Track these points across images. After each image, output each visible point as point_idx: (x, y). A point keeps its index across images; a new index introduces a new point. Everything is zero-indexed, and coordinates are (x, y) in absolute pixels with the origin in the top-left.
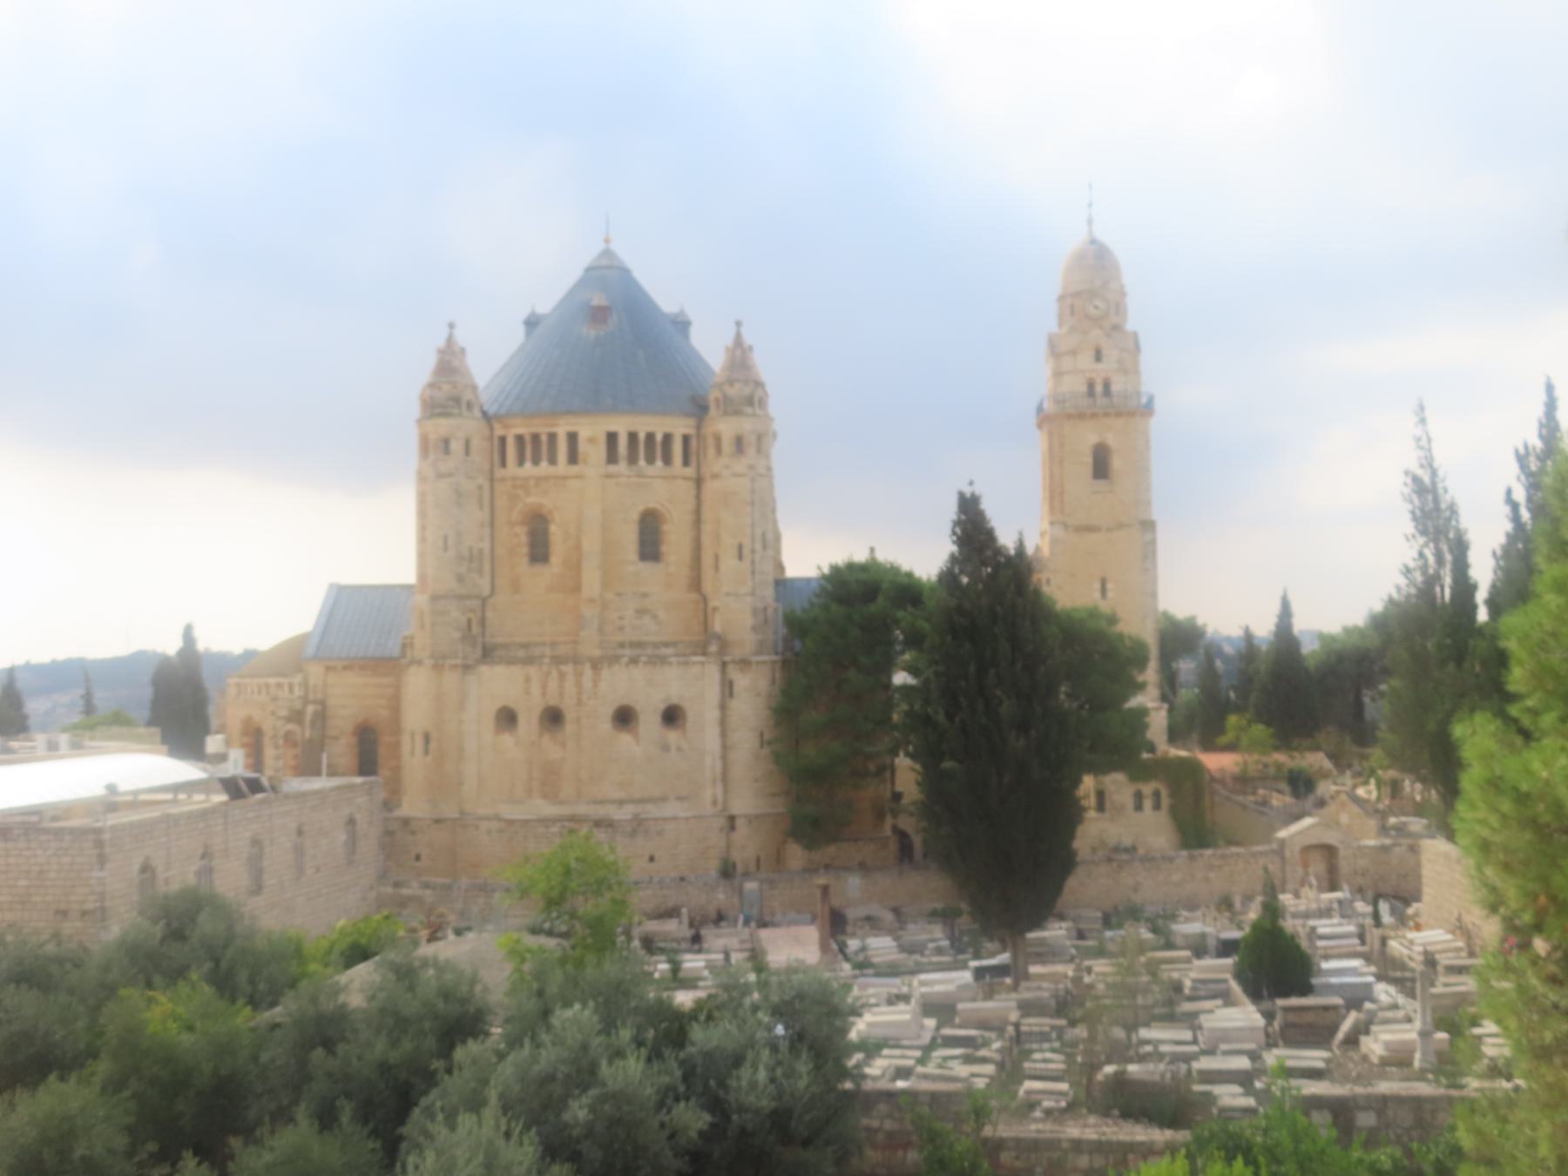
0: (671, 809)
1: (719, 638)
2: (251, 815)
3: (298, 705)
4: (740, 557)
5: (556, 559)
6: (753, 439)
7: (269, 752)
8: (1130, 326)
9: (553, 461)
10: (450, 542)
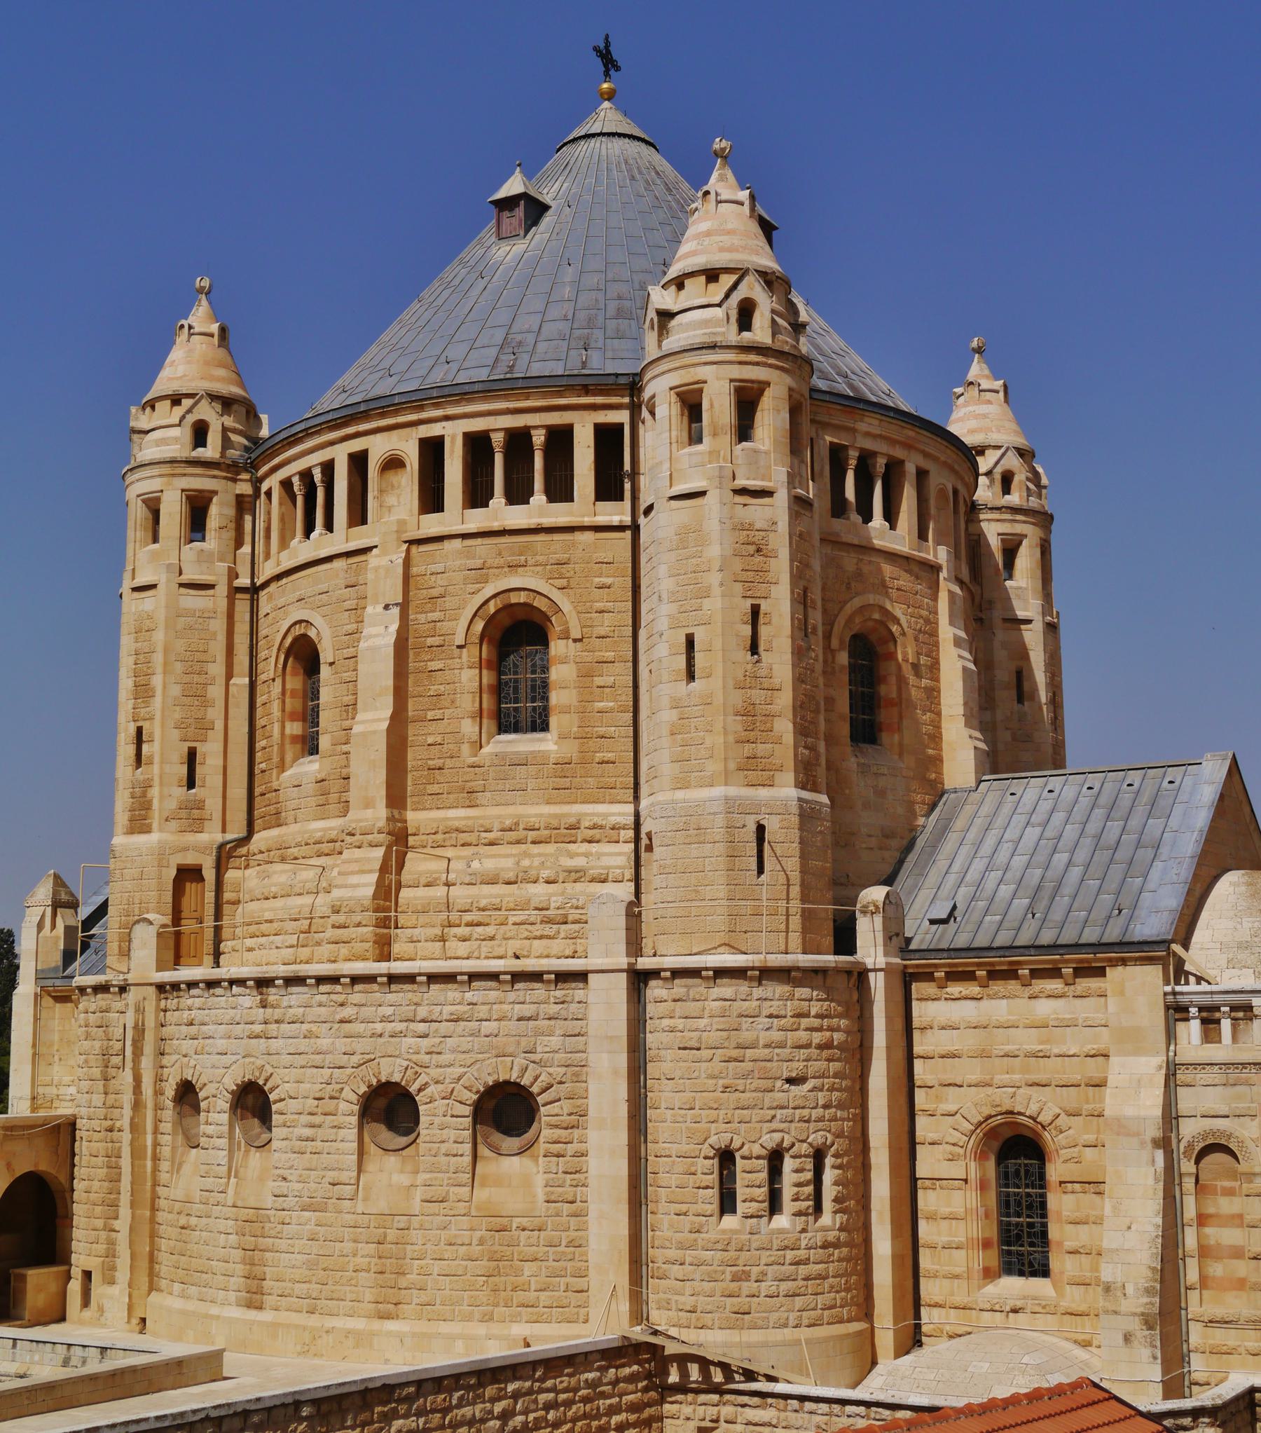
9: (329, 526)
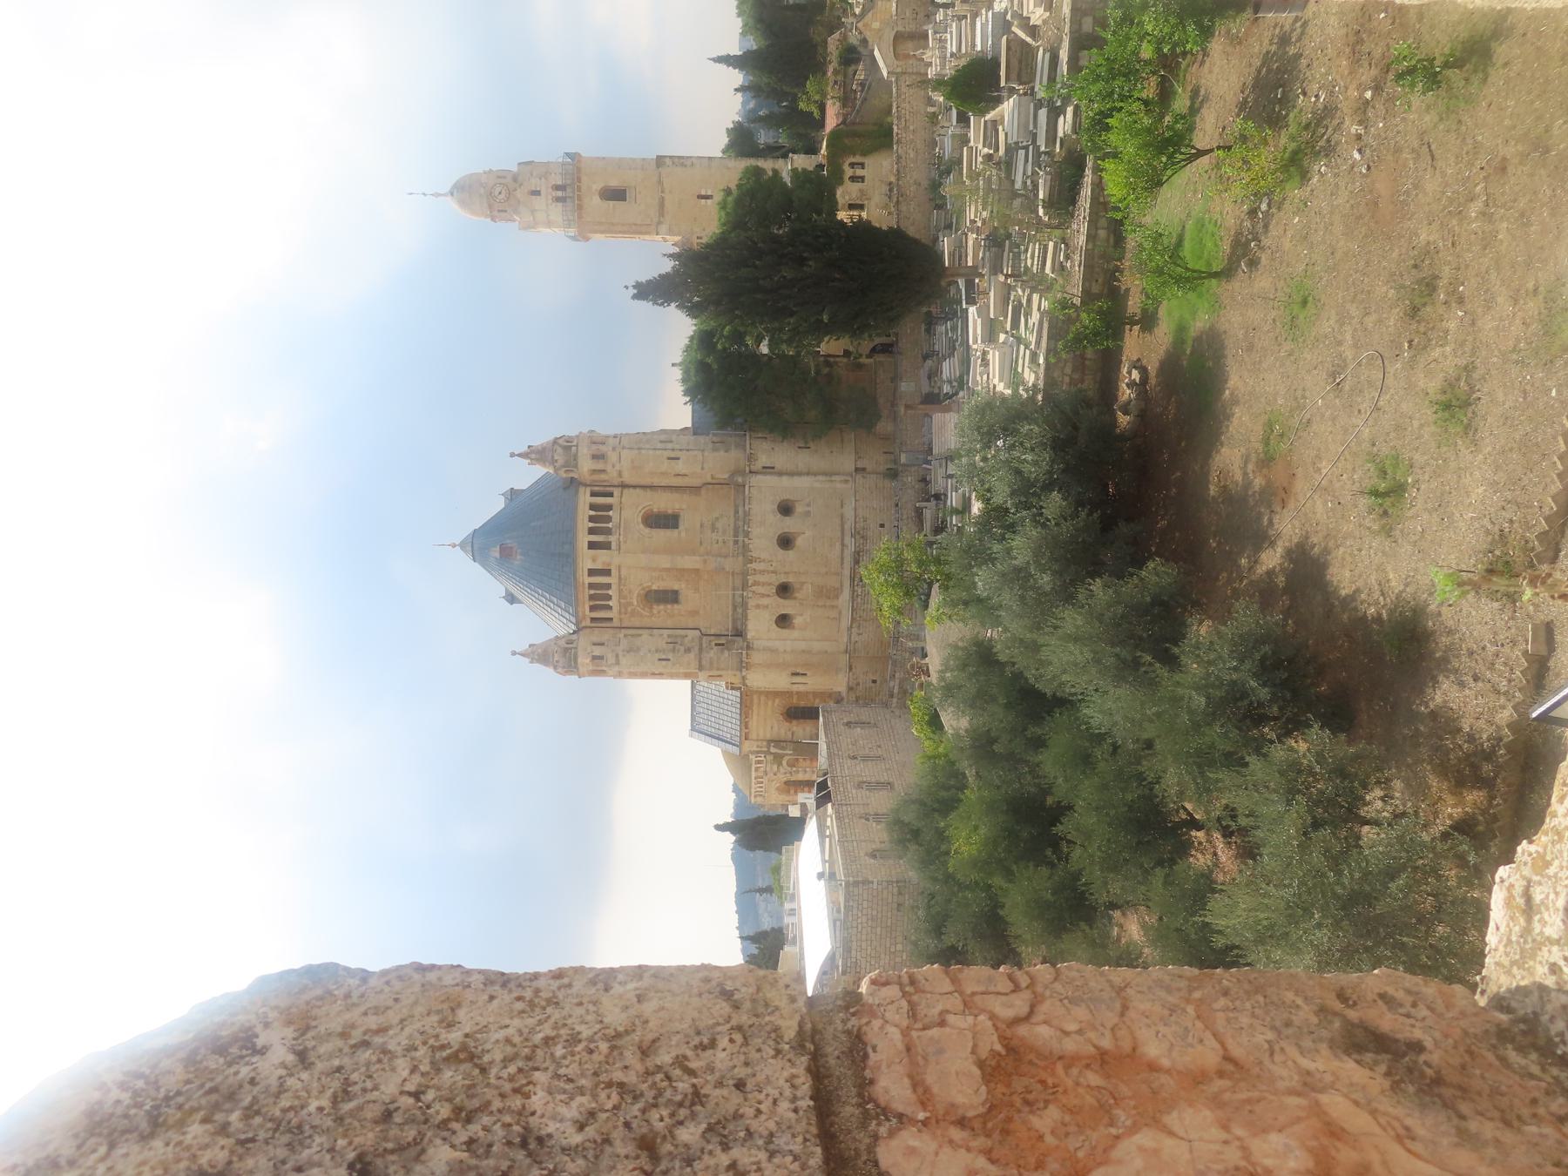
0: (849, 512)
1: (733, 475)
2: (841, 789)
3: (770, 758)
4: (678, 459)
5: (676, 588)
6: (594, 447)
7: (800, 777)
8: (515, 169)
9: (608, 586)
10: (664, 657)
